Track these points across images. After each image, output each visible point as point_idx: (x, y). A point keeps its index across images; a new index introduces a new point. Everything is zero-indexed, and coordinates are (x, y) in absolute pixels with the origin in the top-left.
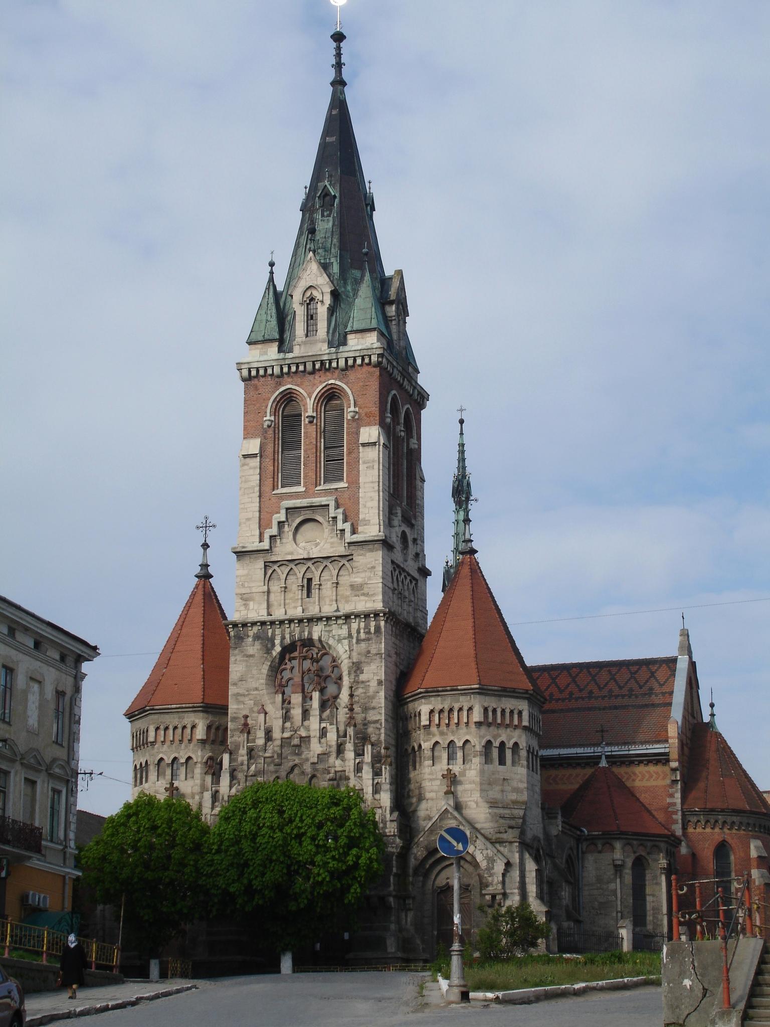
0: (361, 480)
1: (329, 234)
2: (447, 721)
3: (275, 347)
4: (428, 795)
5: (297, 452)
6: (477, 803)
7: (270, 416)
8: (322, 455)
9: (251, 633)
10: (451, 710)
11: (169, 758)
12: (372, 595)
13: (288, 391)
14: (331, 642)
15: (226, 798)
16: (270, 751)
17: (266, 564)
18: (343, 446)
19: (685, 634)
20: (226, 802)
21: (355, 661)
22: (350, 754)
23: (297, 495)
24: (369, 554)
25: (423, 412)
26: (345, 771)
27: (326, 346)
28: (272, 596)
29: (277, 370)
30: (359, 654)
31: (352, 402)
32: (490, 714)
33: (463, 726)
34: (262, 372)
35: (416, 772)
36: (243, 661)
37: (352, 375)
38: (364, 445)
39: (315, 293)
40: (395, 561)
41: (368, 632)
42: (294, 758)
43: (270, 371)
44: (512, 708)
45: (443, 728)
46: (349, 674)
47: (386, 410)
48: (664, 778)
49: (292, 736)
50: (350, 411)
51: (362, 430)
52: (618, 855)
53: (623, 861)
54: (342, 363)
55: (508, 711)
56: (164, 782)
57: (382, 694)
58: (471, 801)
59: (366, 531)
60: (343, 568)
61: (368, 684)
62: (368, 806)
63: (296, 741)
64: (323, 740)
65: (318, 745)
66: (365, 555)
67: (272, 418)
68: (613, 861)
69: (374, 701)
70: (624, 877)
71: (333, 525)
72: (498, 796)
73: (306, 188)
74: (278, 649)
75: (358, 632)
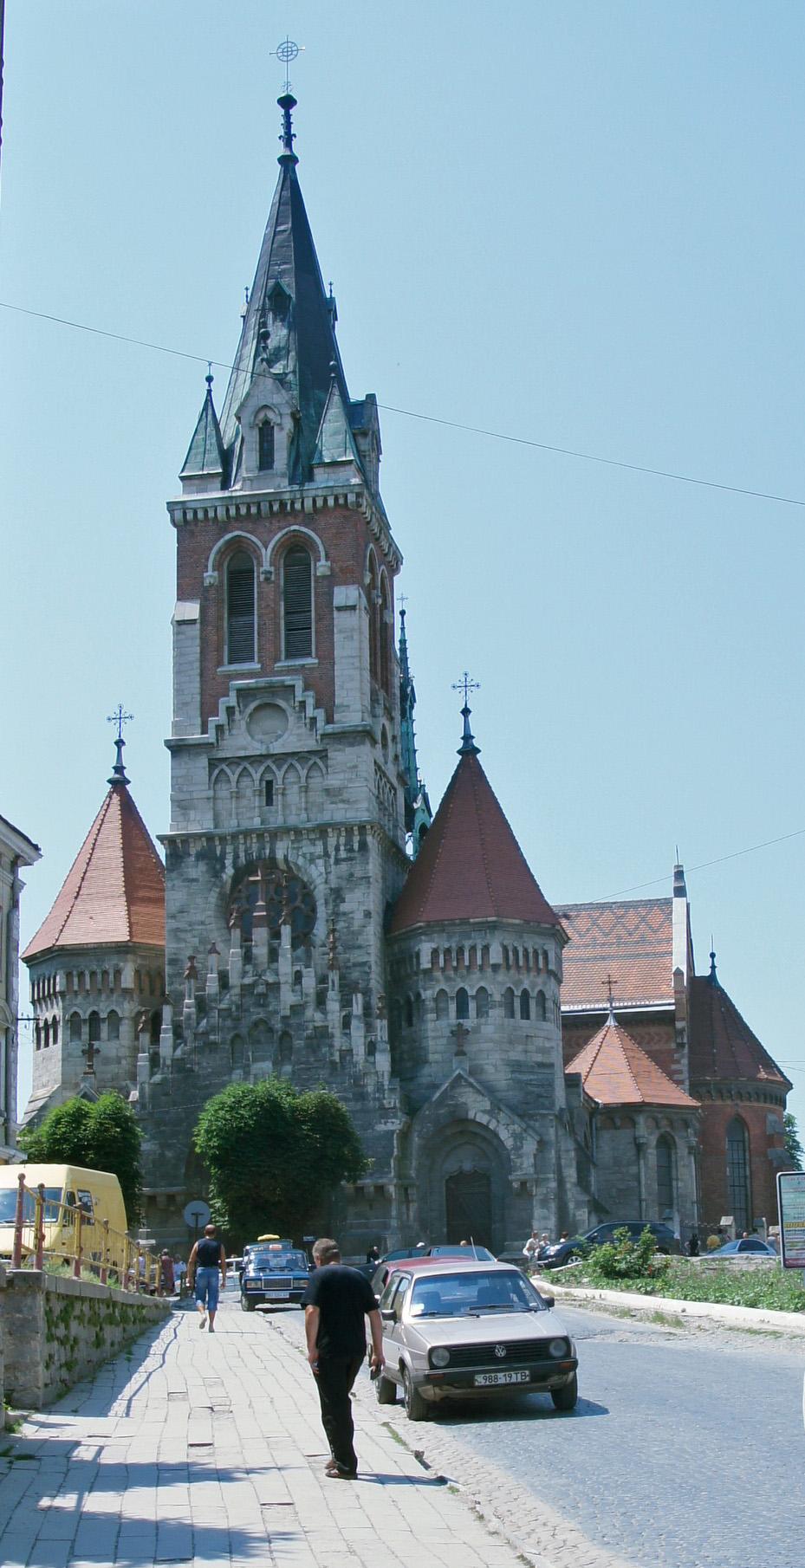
2: (455, 964)
3: (217, 483)
4: (431, 1057)
6: (495, 1066)
7: (214, 570)
8: (282, 622)
9: (193, 851)
10: (461, 950)
11: (85, 1013)
12: (356, 802)
13: (237, 538)
14: (301, 861)
15: (169, 1062)
16: (226, 1002)
18: (310, 611)
20: (168, 1067)
21: (333, 886)
22: (333, 1005)
23: (251, 675)
24: (348, 750)
27: (286, 481)
29: (221, 513)
30: (338, 878)
31: (323, 554)
32: (511, 954)
34: (200, 515)
35: (413, 1029)
36: (185, 886)
37: (322, 521)
38: (339, 609)
39: (271, 415)
41: (351, 850)
42: (260, 1010)
46: (326, 903)
47: (364, 566)
49: (255, 981)
50: (322, 567)
51: (336, 590)
54: (308, 503)
55: (531, 950)
56: (80, 1043)
58: (487, 1064)
59: (344, 720)
60: (314, 768)
61: (351, 915)
62: (360, 1070)
63: (261, 989)
65: (291, 993)
67: (216, 574)
68: (635, 1139)
71: (300, 712)
72: (521, 1057)
73: (247, 289)
74: (230, 871)
75: (337, 849)
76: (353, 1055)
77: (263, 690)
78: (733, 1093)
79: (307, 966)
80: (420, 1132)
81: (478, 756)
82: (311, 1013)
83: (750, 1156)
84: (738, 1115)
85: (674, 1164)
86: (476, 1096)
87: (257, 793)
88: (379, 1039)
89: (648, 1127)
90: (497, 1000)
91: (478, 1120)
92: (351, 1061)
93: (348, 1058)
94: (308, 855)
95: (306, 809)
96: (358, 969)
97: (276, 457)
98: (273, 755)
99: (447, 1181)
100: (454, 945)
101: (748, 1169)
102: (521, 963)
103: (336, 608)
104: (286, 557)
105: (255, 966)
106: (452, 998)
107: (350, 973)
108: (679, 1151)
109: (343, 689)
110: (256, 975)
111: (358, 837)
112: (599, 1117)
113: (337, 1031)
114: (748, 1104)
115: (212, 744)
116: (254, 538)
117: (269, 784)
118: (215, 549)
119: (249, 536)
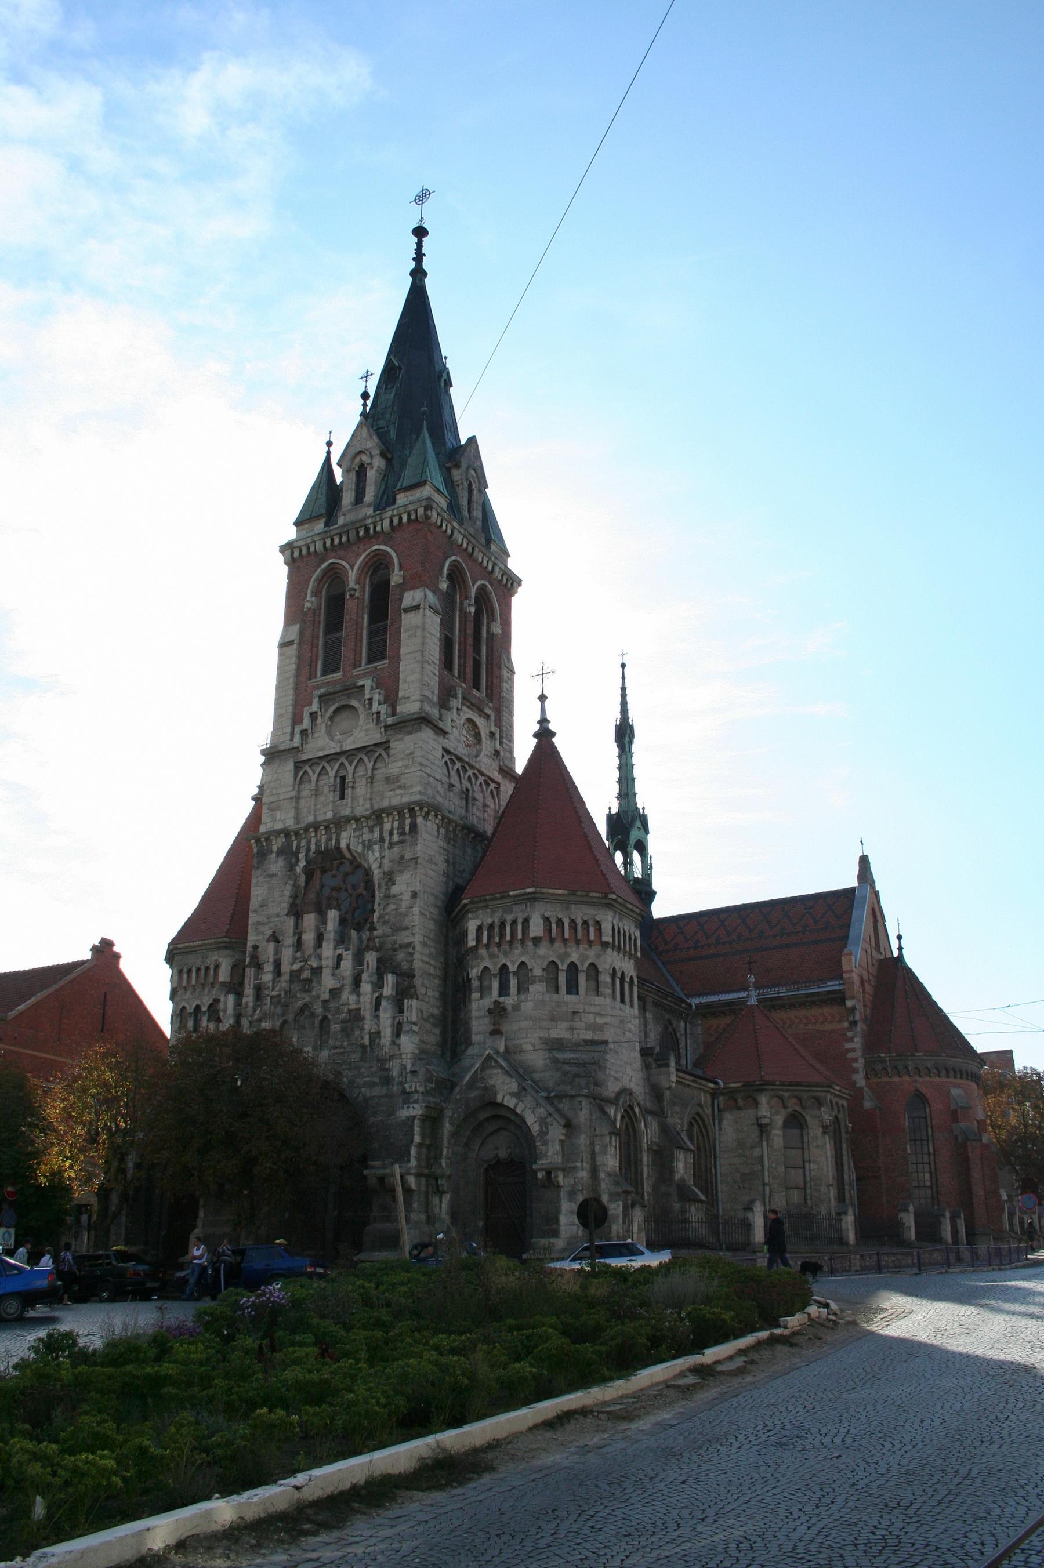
0: (402, 651)
1: (390, 403)
2: (497, 939)
4: (475, 1038)
5: (338, 635)
6: (534, 1045)
8: (365, 632)
9: (275, 848)
10: (503, 925)
11: (190, 1006)
12: (411, 786)
17: (298, 765)
19: (864, 861)
21: (386, 869)
25: (515, 600)
26: (359, 1009)
27: (370, 511)
28: (303, 803)
29: (319, 546)
32: (554, 926)
34: (304, 551)
39: (365, 458)
40: (452, 750)
41: (402, 833)
42: (303, 995)
43: (312, 549)
45: (495, 949)
47: (441, 573)
48: (840, 1021)
49: (302, 967)
50: (396, 578)
51: (406, 595)
53: (771, 1119)
54: (386, 523)
55: (579, 922)
57: (416, 910)
61: (400, 897)
63: (306, 974)
64: (338, 971)
65: (330, 978)
66: (403, 739)
69: (407, 919)
74: (302, 863)
75: (391, 834)
76: (380, 1037)
77: (341, 694)
78: (910, 1068)
79: (347, 949)
81: (554, 740)
82: (348, 997)
83: (932, 1131)
84: (917, 1090)
85: (805, 1147)
86: (505, 1077)
87: (332, 788)
88: (405, 1020)
91: (505, 1103)
92: (379, 1044)
93: (377, 1041)
95: (371, 799)
96: (405, 950)
97: (367, 490)
99: (486, 1169)
100: (496, 921)
101: (930, 1144)
102: (567, 935)
103: (404, 610)
104: (372, 575)
105: (303, 953)
106: (495, 975)
107: (396, 955)
108: (810, 1131)
109: (405, 682)
112: (721, 1098)
113: (367, 1013)
114: (928, 1079)
115: (297, 748)
116: (343, 563)
117: (343, 778)
118: (314, 578)
119: (340, 561)
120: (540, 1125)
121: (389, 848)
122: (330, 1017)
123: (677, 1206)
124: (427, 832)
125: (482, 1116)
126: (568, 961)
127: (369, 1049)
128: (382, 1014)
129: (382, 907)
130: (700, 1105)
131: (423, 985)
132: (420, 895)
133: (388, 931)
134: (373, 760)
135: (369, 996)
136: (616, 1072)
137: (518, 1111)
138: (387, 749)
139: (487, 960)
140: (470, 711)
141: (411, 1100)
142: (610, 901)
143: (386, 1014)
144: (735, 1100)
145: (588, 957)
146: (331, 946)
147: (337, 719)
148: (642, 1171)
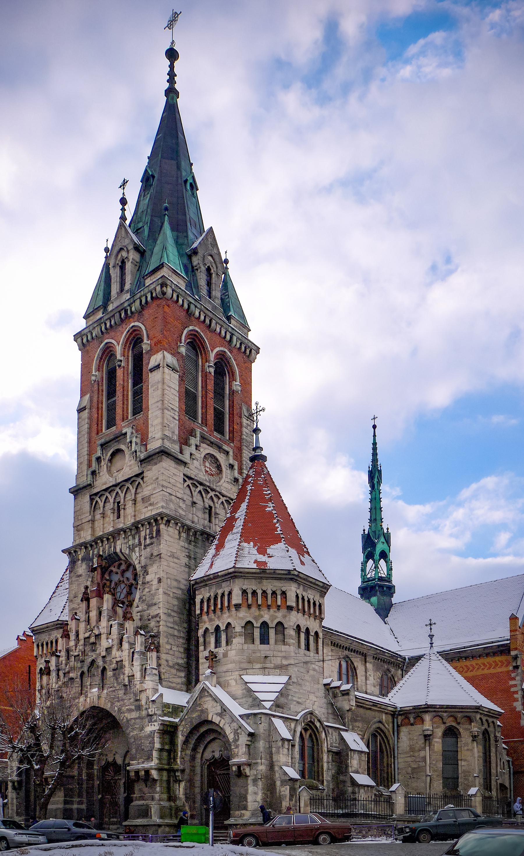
2: (212, 608)
21: (143, 565)
26: (122, 661)
30: (145, 559)
33: (226, 610)
40: (193, 477)
41: (152, 538)
44: (274, 589)
45: (212, 615)
52: (428, 725)
55: (269, 592)
57: (161, 591)
61: (151, 583)
69: (155, 598)
70: (434, 746)
80: (182, 731)
89: (433, 723)
90: (238, 631)
91: (213, 721)
94: (131, 546)
96: (154, 619)
98: (119, 484)
107: (150, 623)
110: (91, 631)
111: (156, 527)
112: (400, 717)
113: (126, 663)
120: (234, 735)
121: (144, 549)
122: (106, 667)
123: (350, 789)
124: (168, 535)
125: (203, 730)
126: (261, 621)
127: (128, 687)
128: (134, 663)
129: (141, 590)
130: (380, 722)
131: (167, 643)
132: (164, 580)
133: (145, 607)
134: (135, 486)
135: (127, 651)
136: (299, 698)
137: (221, 725)
138: (142, 479)
139: (208, 623)
140: (210, 448)
141: (153, 720)
142: (292, 577)
143: (137, 663)
144: (408, 718)
145: (276, 617)
146: (106, 619)
147: (114, 460)
148: (322, 766)
